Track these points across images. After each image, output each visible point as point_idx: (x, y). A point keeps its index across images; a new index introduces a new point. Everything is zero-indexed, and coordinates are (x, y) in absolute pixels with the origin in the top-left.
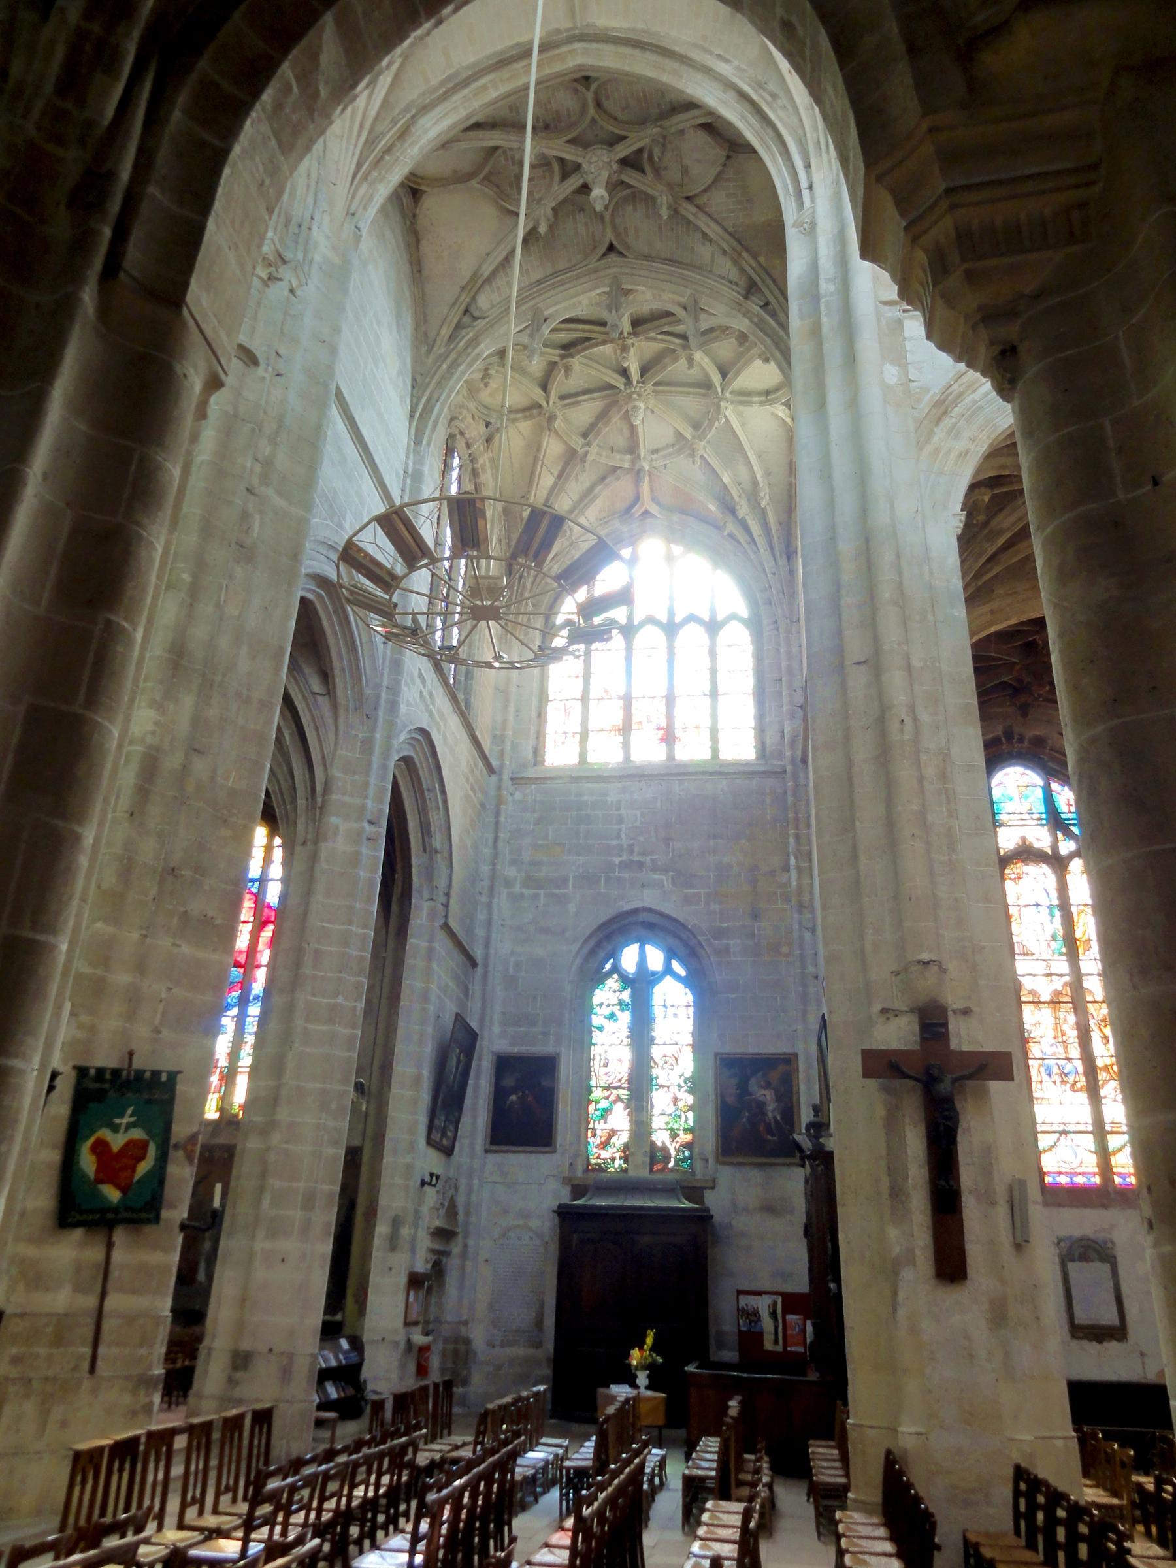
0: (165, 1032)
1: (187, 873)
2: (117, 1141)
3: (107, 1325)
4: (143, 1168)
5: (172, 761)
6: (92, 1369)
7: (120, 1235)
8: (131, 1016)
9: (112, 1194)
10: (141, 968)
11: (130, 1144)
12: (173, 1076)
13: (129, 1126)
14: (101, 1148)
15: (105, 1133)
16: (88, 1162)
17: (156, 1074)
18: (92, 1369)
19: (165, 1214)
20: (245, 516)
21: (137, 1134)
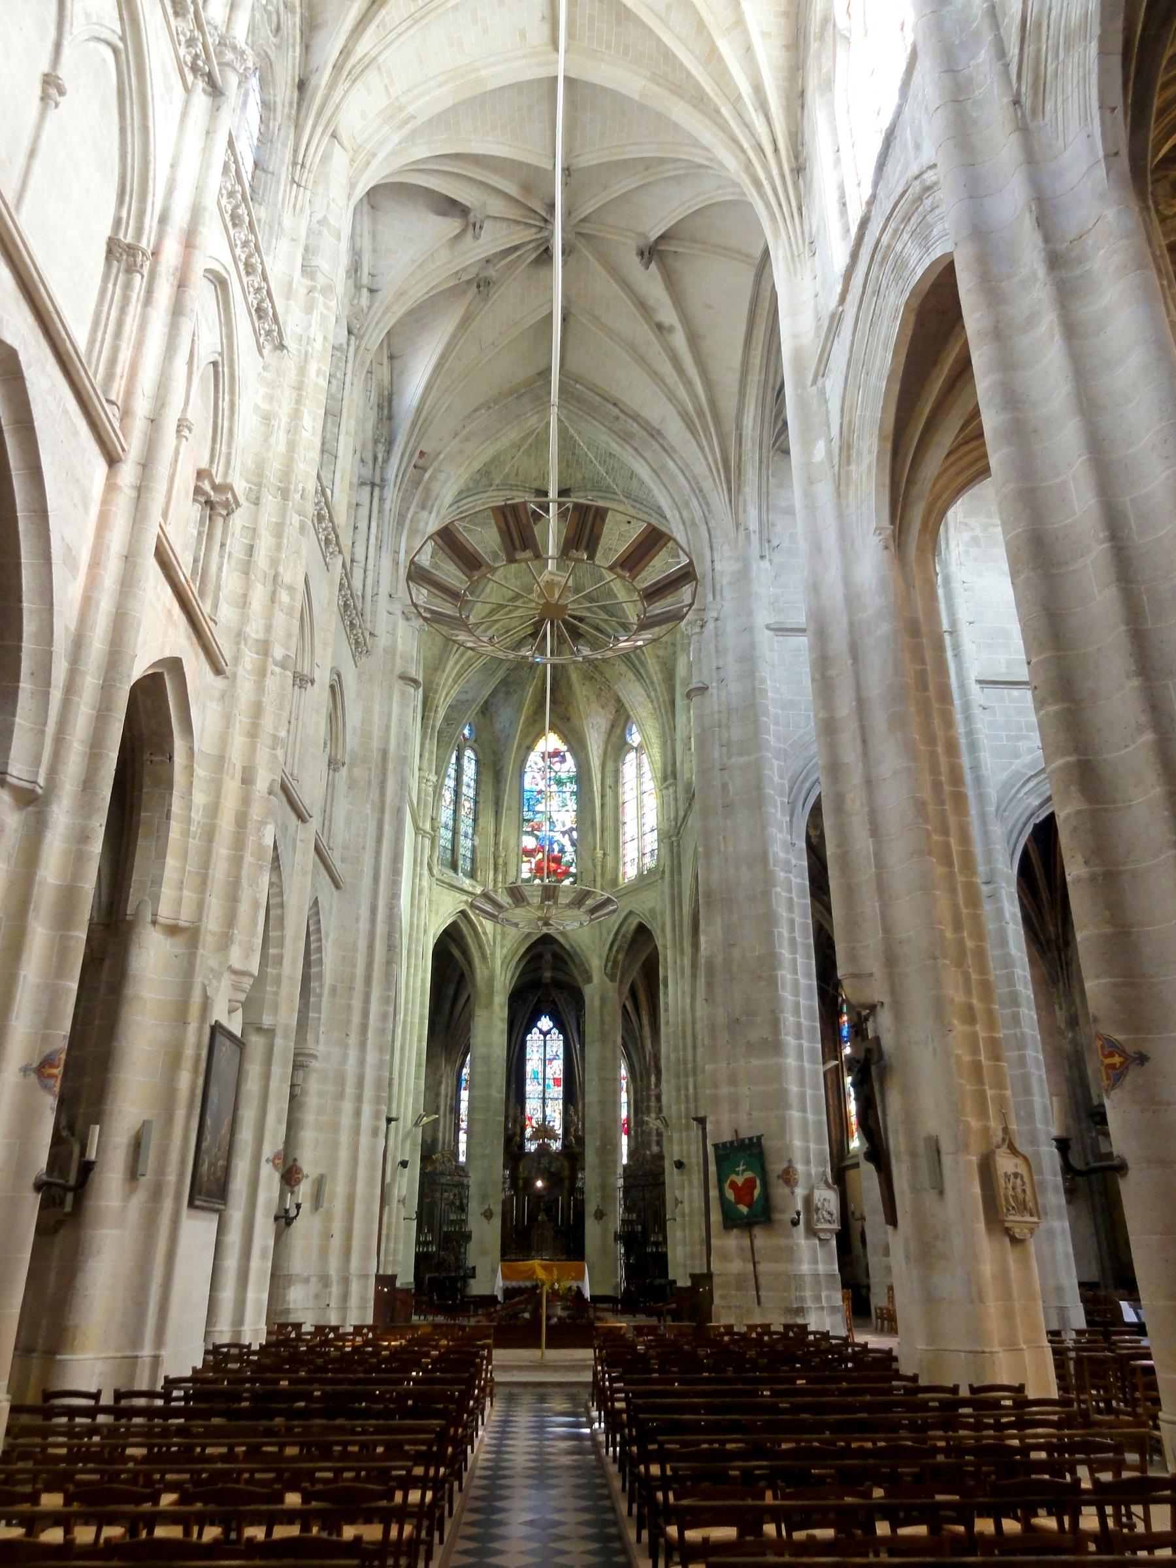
0: (754, 1113)
1: (744, 1019)
2: (740, 1180)
3: (762, 1280)
4: (757, 1192)
5: (719, 960)
6: (759, 1303)
7: (757, 1231)
8: (734, 1109)
9: (744, 1209)
10: (733, 1081)
11: (747, 1181)
12: (759, 1138)
13: (744, 1171)
14: (733, 1185)
15: (733, 1177)
16: (730, 1194)
17: (751, 1139)
18: (759, 1303)
19: (776, 1216)
20: (724, 786)
21: (749, 1174)
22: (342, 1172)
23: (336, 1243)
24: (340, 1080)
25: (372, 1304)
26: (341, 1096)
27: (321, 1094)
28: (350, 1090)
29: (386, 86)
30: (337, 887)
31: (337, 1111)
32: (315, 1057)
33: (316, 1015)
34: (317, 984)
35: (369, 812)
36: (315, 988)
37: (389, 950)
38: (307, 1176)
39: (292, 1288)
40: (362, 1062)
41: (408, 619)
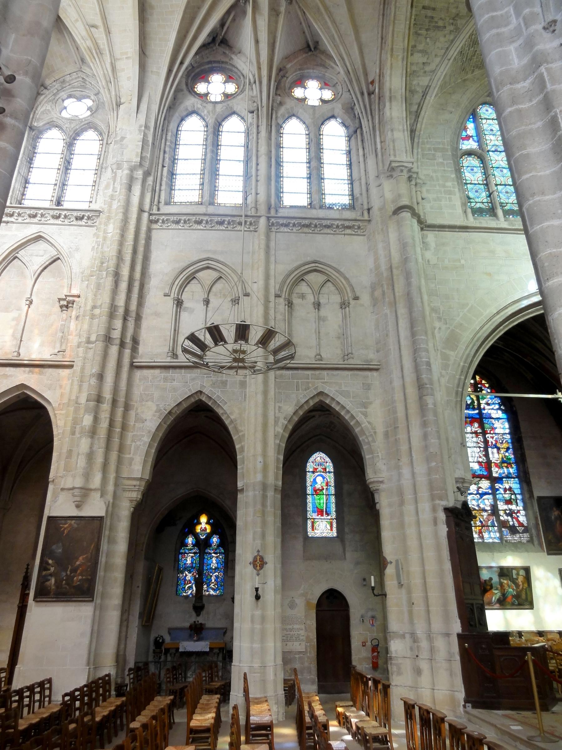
22: (414, 556)
23: (419, 608)
24: (401, 493)
25: (458, 658)
26: (402, 503)
27: (390, 505)
28: (409, 496)
29: (126, 58)
30: (377, 370)
31: (402, 514)
32: (382, 482)
33: (371, 456)
34: (364, 437)
35: (388, 311)
36: (363, 440)
37: (419, 389)
38: (391, 563)
39: (392, 642)
40: (413, 474)
41: (391, 176)
